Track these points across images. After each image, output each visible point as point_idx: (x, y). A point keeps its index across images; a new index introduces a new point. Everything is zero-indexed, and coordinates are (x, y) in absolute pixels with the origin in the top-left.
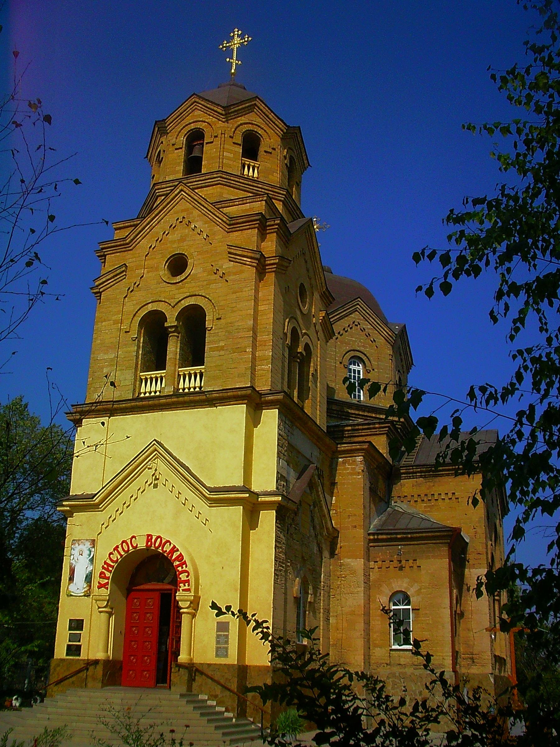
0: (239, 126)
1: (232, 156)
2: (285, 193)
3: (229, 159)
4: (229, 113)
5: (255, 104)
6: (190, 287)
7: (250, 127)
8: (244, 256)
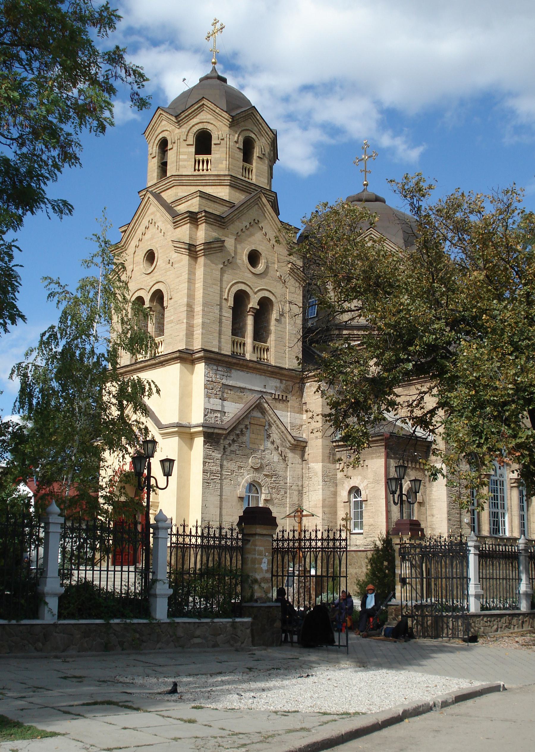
0: (191, 128)
1: (185, 157)
2: (229, 178)
3: (184, 160)
4: (181, 120)
5: (203, 104)
6: (157, 276)
7: (200, 126)
8: (181, 248)
